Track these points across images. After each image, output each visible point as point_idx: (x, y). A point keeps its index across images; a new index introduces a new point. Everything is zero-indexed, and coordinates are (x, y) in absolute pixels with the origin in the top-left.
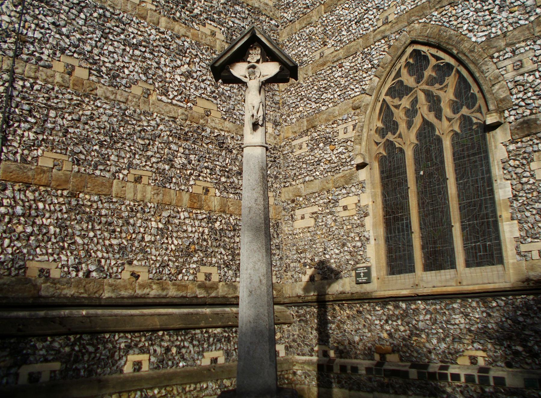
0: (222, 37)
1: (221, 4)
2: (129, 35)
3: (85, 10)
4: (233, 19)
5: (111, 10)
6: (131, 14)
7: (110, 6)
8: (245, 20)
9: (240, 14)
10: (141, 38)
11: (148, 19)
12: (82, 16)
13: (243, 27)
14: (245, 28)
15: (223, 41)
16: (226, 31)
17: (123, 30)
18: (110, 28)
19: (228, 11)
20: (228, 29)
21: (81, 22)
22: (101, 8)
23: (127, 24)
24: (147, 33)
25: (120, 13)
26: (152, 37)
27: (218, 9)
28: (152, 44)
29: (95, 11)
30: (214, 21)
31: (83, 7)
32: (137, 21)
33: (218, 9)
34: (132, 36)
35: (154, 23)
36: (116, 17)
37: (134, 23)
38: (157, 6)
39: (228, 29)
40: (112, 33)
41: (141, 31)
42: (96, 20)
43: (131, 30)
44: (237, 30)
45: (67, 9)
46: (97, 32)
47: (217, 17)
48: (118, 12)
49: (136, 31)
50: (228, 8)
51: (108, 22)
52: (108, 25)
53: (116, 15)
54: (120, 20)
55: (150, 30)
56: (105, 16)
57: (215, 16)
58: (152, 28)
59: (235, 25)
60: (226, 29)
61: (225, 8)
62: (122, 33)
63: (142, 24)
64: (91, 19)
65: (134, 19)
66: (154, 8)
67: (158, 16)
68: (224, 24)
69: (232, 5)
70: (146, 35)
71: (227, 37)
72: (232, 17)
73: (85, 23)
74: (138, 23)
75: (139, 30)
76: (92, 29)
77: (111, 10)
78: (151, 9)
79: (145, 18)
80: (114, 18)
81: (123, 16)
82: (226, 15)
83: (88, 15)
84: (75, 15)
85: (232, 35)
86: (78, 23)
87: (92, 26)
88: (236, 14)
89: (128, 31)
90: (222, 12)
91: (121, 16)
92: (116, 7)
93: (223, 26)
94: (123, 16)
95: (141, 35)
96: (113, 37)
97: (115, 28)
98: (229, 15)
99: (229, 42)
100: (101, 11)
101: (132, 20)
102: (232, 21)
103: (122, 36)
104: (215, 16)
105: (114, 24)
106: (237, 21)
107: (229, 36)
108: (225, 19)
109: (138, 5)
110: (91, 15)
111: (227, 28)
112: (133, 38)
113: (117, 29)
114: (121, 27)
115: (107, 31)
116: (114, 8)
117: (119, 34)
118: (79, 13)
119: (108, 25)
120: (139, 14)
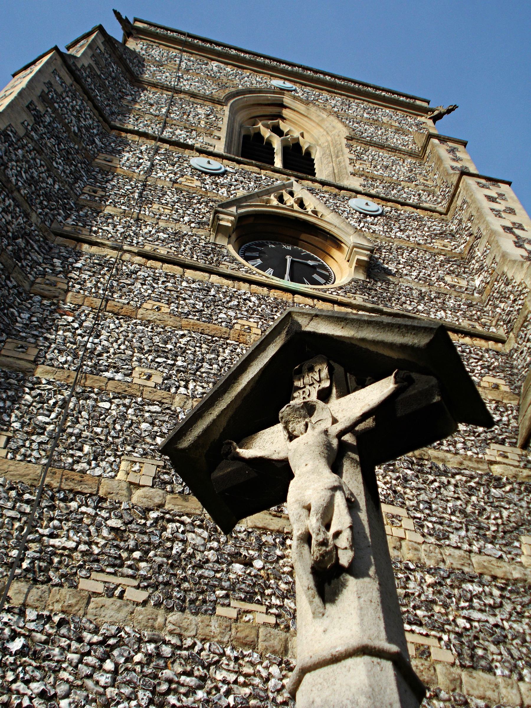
0: (449, 657)
1: (429, 586)
2: (218, 689)
3: (116, 653)
4: (465, 613)
5: (174, 640)
6: (219, 642)
7: (171, 633)
8: (497, 611)
9: (480, 598)
10: (247, 691)
11: (261, 646)
12: (109, 665)
13: (496, 626)
14: (503, 628)
15: (453, 665)
16: (454, 641)
17: (203, 679)
18: (170, 681)
19: (449, 596)
20: (459, 635)
21: (104, 679)
22: (150, 641)
23: (210, 665)
24: (261, 677)
25: (195, 644)
26: (272, 683)
27: (423, 598)
28: (274, 700)
29: (139, 650)
30: (421, 625)
31: (113, 647)
32: (235, 654)
33: (423, 598)
34: (224, 688)
35: (274, 652)
36: (185, 653)
37: (229, 659)
38: (278, 616)
39: (459, 635)
40: (176, 692)
41: (246, 675)
42: (138, 668)
43: (219, 676)
44: (481, 635)
45: (75, 657)
46: (140, 694)
47: (425, 613)
48: (189, 642)
49: (232, 677)
50: (446, 590)
51: (166, 667)
52: (167, 673)
53: (186, 649)
54: (193, 659)
55: (267, 668)
56: (159, 655)
57: (419, 613)
58: (272, 664)
59: (476, 624)
60: (452, 636)
61: (440, 592)
62: (200, 687)
63: (247, 659)
64: (126, 669)
65: (228, 651)
66: (272, 620)
67: (283, 635)
68: (447, 627)
69: (457, 583)
70: (257, 681)
71: (459, 655)
72: (463, 608)
73: (114, 680)
74: (236, 659)
75: (239, 673)
76: (126, 691)
77: (174, 640)
78: (265, 624)
79: (253, 646)
80: (180, 657)
81: (202, 650)
82: (445, 606)
83: (122, 660)
84: (94, 667)
85: (473, 648)
86: (97, 683)
87: (129, 683)
88: (471, 601)
89: (213, 680)
90: (434, 602)
91: (197, 649)
92: (186, 634)
93: (443, 631)
94: (202, 650)
95: (245, 685)
96: (179, 700)
97: (183, 678)
98: (453, 606)
99: (468, 663)
100: (151, 647)
101: (223, 654)
102: (464, 617)
103: (201, 694)
104: (419, 613)
105: (180, 670)
106: (476, 615)
107: (466, 651)
108: (447, 614)
109: (236, 620)
110: (129, 659)
111: (457, 633)
112: (228, 693)
113: (188, 679)
114: (196, 673)
115: (164, 687)
116: (180, 636)
117: (192, 691)
118: (102, 660)
119: (167, 673)
120: (237, 639)
